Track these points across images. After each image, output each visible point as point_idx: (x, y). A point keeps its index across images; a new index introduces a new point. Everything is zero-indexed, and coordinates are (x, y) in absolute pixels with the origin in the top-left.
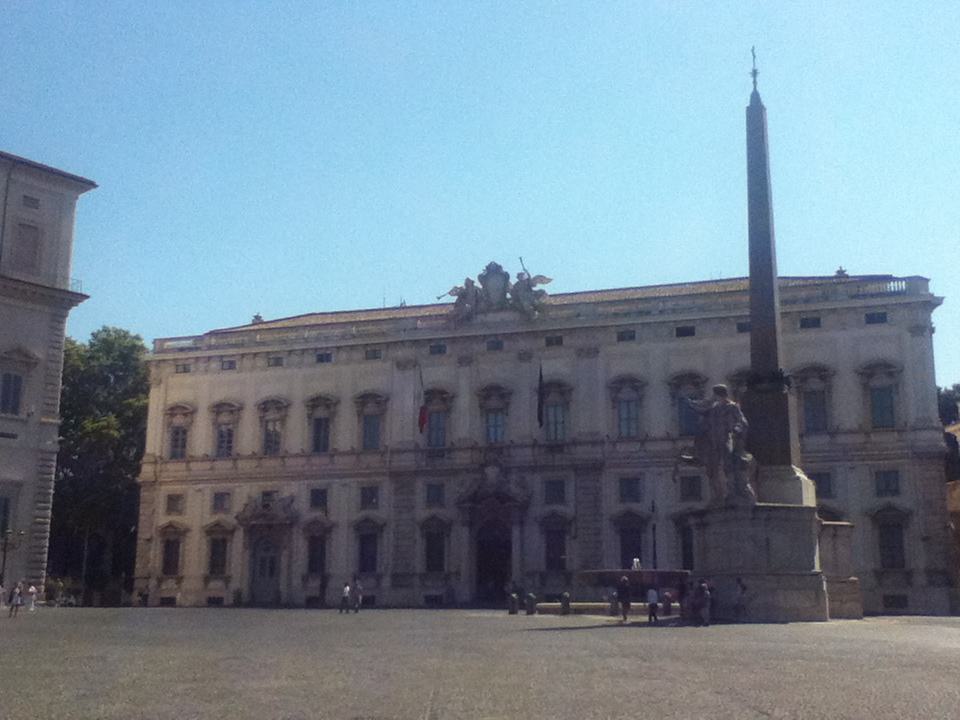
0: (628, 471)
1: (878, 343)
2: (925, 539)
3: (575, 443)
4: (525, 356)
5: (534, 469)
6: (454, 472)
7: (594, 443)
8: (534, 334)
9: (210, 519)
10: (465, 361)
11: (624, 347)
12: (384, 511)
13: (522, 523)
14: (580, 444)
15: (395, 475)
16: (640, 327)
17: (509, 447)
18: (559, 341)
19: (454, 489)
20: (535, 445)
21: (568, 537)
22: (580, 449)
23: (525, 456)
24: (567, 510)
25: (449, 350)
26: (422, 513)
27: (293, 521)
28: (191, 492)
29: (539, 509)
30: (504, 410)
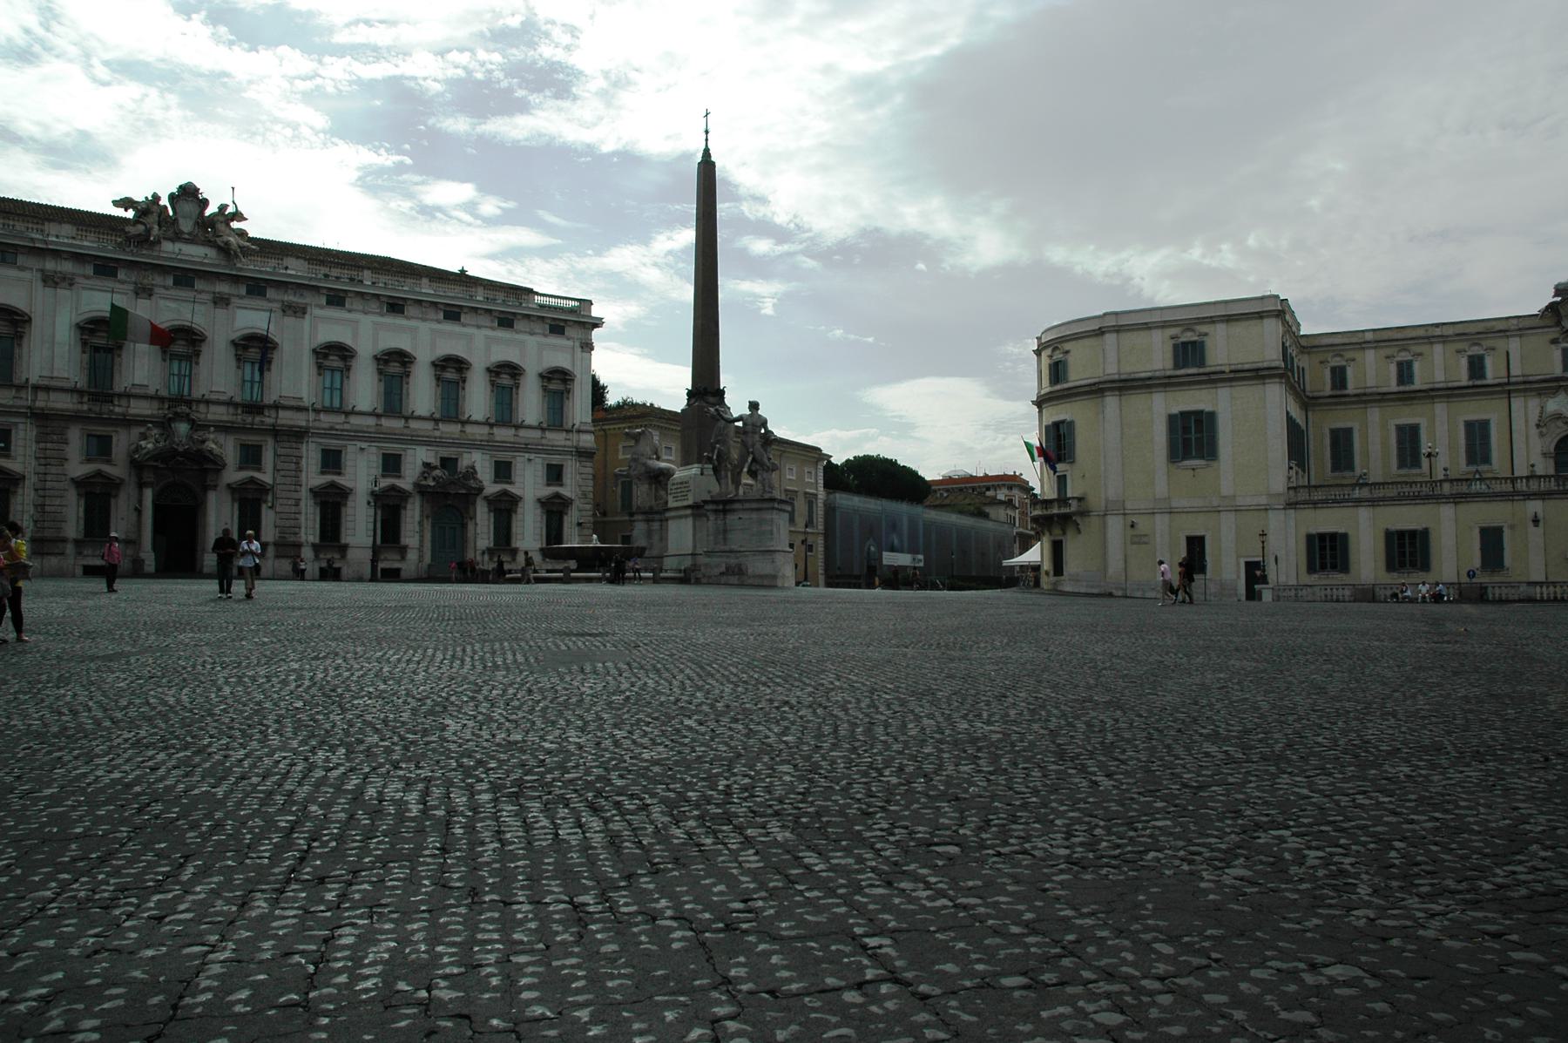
0: (334, 443)
1: (556, 354)
2: (579, 524)
4: (221, 301)
6: (127, 422)
8: (236, 279)
20: (230, 403)
21: (264, 507)
23: (218, 413)
24: (266, 478)
25: (121, 275)
26: (78, 468)
30: (193, 356)
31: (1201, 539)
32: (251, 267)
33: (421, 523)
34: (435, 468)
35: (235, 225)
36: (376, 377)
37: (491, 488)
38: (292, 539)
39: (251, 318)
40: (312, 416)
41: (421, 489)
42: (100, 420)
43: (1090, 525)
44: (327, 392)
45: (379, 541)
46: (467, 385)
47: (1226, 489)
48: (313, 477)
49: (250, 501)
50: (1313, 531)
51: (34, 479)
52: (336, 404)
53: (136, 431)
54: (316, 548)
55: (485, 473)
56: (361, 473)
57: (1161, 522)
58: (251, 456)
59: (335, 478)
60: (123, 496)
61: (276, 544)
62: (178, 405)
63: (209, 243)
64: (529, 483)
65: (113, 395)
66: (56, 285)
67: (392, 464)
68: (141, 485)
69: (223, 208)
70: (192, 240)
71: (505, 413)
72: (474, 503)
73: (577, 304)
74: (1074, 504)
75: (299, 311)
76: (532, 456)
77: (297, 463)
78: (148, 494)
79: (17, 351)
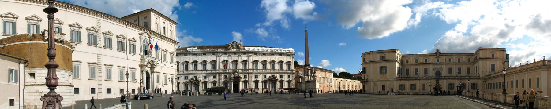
5: (241, 73)
23: (240, 71)
24: (247, 80)
31: (384, 85)
37: (280, 79)
39: (244, 58)
42: (225, 73)
43: (368, 83)
45: (263, 88)
47: (388, 78)
49: (245, 83)
50: (400, 84)
56: (261, 78)
57: (379, 82)
58: (245, 77)
59: (257, 79)
62: (235, 71)
64: (285, 78)
67: (265, 76)
69: (239, 43)
71: (281, 68)
74: (366, 80)
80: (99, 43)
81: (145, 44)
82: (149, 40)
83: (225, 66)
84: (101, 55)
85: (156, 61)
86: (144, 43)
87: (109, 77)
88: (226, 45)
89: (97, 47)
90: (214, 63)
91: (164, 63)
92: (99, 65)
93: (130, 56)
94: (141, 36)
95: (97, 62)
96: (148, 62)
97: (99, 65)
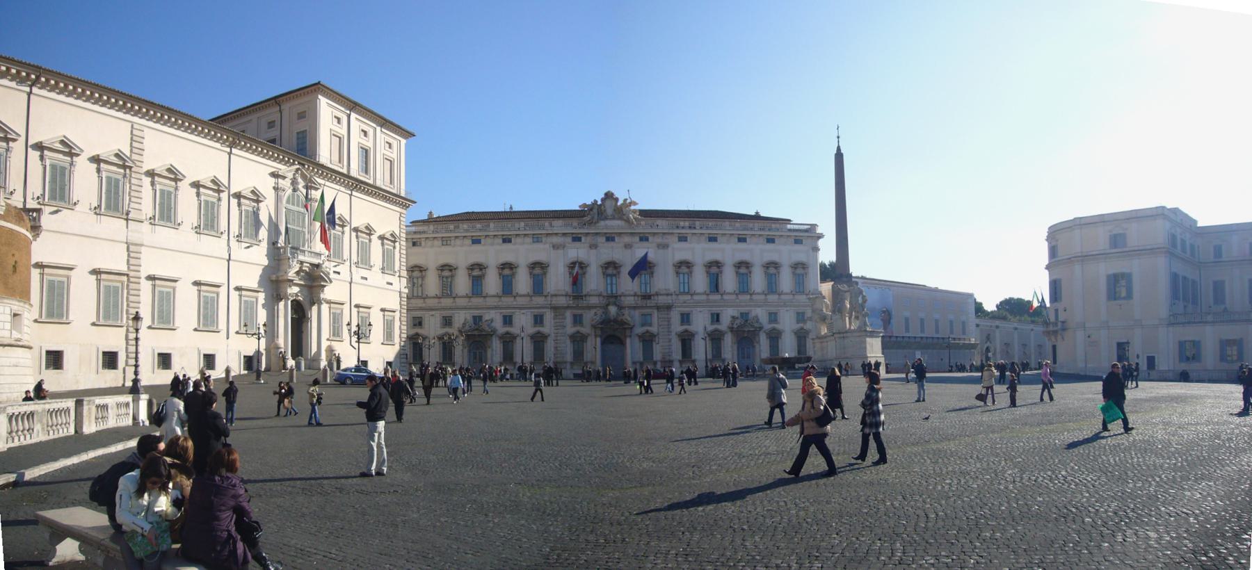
0: (686, 310)
3: (657, 294)
4: (628, 246)
6: (589, 308)
7: (667, 295)
9: (441, 331)
10: (593, 246)
11: (683, 245)
12: (547, 328)
13: (630, 336)
14: (661, 295)
15: (555, 308)
16: (690, 235)
17: (620, 296)
18: (647, 239)
19: (589, 317)
20: (635, 295)
22: (660, 297)
23: (629, 301)
24: (654, 329)
26: (571, 329)
27: (494, 331)
28: (427, 315)
29: (639, 330)
30: (617, 275)
32: (644, 227)
33: (732, 347)
34: (737, 318)
35: (633, 208)
36: (705, 275)
37: (768, 326)
38: (667, 358)
40: (674, 297)
41: (731, 329)
42: (577, 307)
44: (682, 285)
46: (752, 275)
48: (677, 327)
51: (553, 335)
52: (686, 290)
53: (593, 311)
54: (681, 362)
55: (764, 319)
60: (589, 339)
61: (661, 362)
63: (621, 219)
65: (582, 296)
66: (558, 248)
68: (596, 336)
69: (625, 200)
70: (614, 218)
72: (758, 335)
73: (809, 227)
75: (664, 246)
76: (788, 308)
77: (669, 321)
78: (599, 340)
79: (544, 280)
80: (136, 206)
81: (295, 208)
82: (307, 194)
83: (576, 281)
84: (142, 245)
85: (329, 266)
86: (290, 207)
87: (164, 319)
88: (580, 206)
89: (127, 220)
90: (538, 270)
91: (358, 273)
92: (132, 280)
93: (239, 251)
94: (280, 181)
95: (124, 268)
96: (301, 268)
97: (132, 280)
